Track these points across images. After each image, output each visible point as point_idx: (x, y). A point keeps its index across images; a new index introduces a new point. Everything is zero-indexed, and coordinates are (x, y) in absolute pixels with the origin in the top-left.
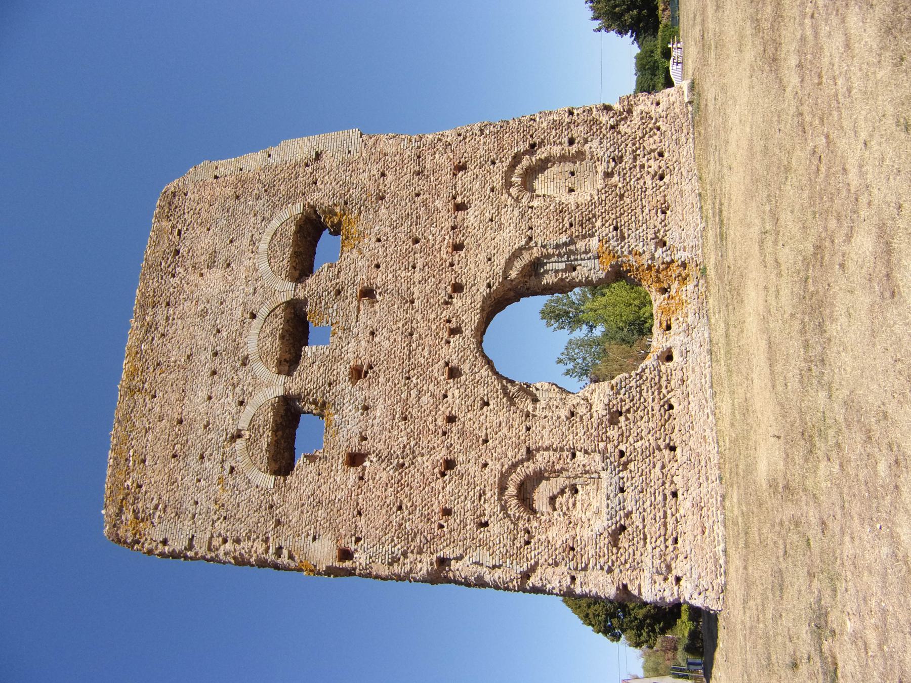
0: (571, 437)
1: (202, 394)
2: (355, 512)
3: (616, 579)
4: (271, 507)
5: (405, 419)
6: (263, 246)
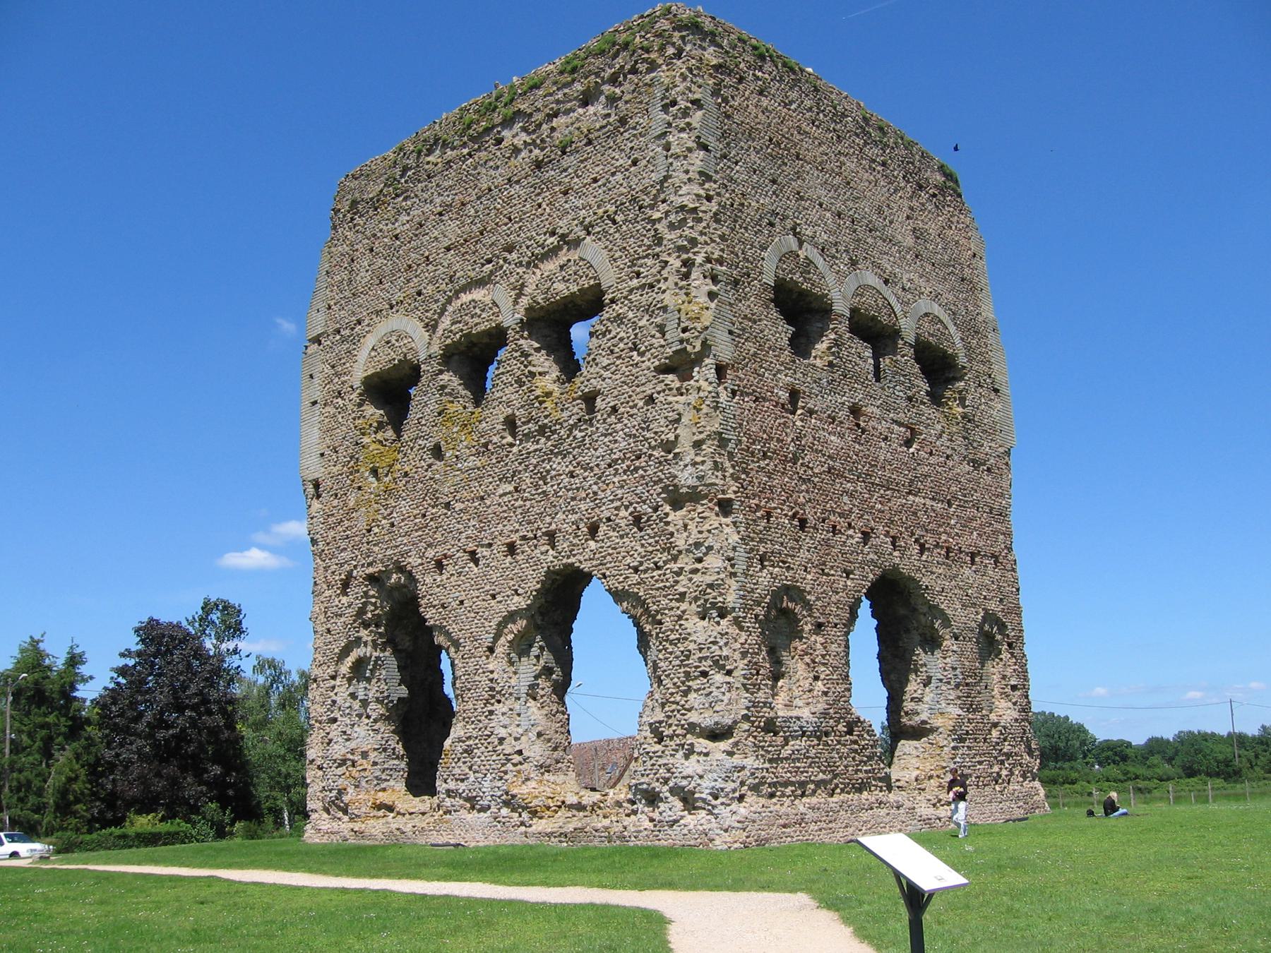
6: (937, 310)
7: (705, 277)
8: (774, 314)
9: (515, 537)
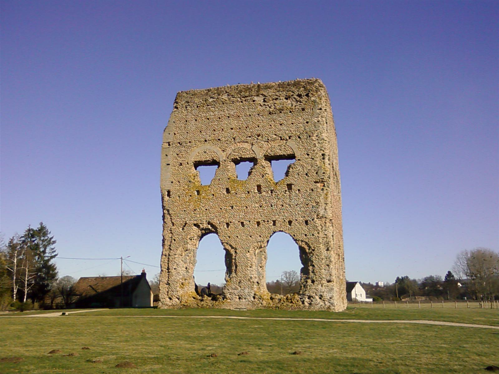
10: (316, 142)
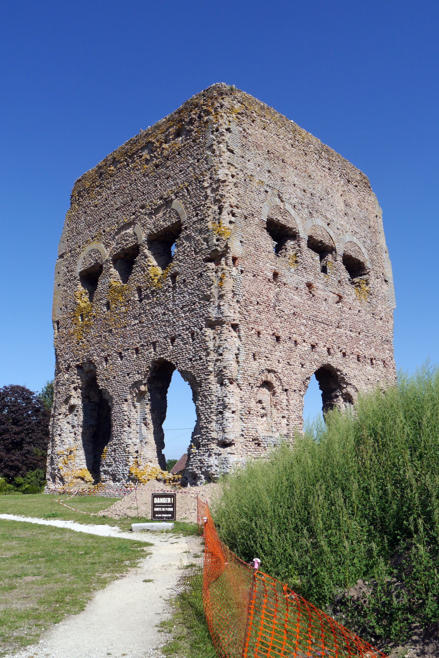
0: (293, 417)
1: (296, 180)
2: (255, 273)
3: (237, 440)
4: (253, 215)
5: (294, 314)
6: (355, 240)
7: (229, 214)
8: (266, 234)
9: (138, 345)
10: (209, 191)
